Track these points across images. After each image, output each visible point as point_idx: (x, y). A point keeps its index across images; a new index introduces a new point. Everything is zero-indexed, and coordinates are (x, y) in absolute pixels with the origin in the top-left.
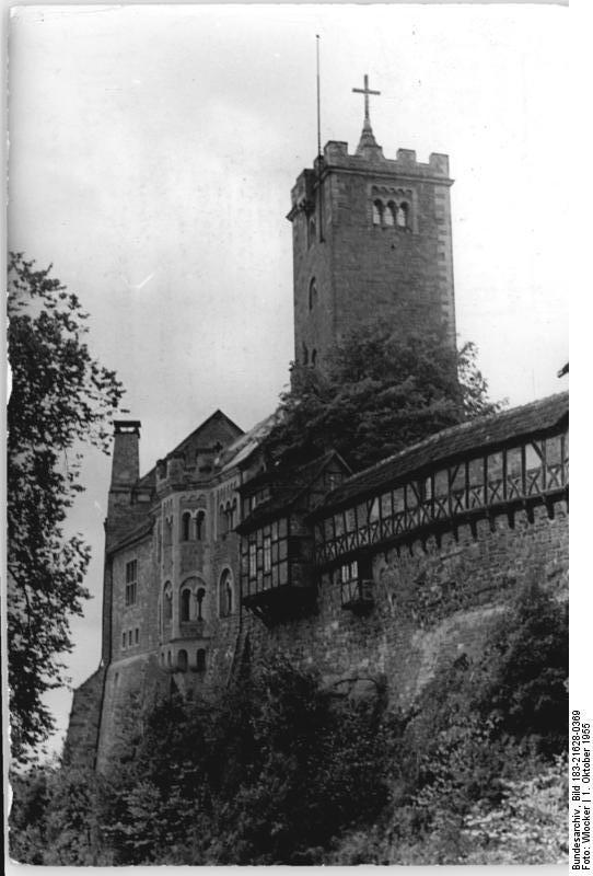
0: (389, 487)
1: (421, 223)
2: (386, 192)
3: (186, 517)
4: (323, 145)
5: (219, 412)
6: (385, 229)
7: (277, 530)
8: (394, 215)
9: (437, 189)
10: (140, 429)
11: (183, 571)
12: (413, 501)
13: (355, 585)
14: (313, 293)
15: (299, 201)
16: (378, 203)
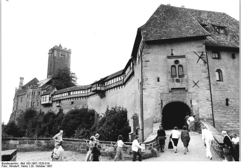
0: (65, 93)
1: (67, 58)
2: (63, 53)
3: (33, 92)
4: (55, 45)
5: (35, 78)
6: (62, 58)
7: (48, 96)
8: (63, 56)
9: (69, 54)
10: (24, 79)
11: (32, 99)
12: (67, 95)
13: (58, 104)
14: (51, 65)
15: (50, 52)
16: (61, 54)
